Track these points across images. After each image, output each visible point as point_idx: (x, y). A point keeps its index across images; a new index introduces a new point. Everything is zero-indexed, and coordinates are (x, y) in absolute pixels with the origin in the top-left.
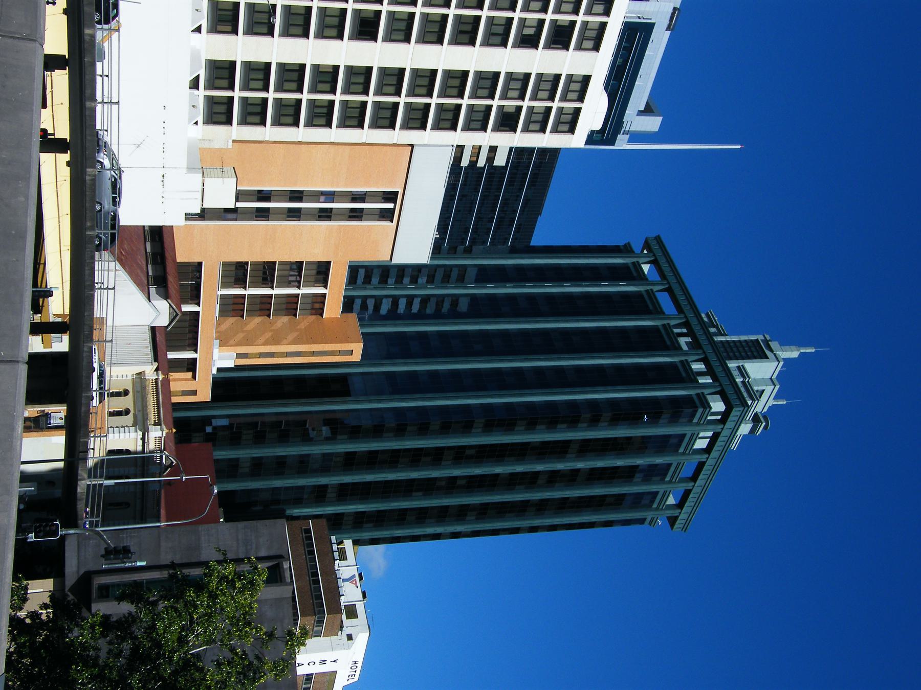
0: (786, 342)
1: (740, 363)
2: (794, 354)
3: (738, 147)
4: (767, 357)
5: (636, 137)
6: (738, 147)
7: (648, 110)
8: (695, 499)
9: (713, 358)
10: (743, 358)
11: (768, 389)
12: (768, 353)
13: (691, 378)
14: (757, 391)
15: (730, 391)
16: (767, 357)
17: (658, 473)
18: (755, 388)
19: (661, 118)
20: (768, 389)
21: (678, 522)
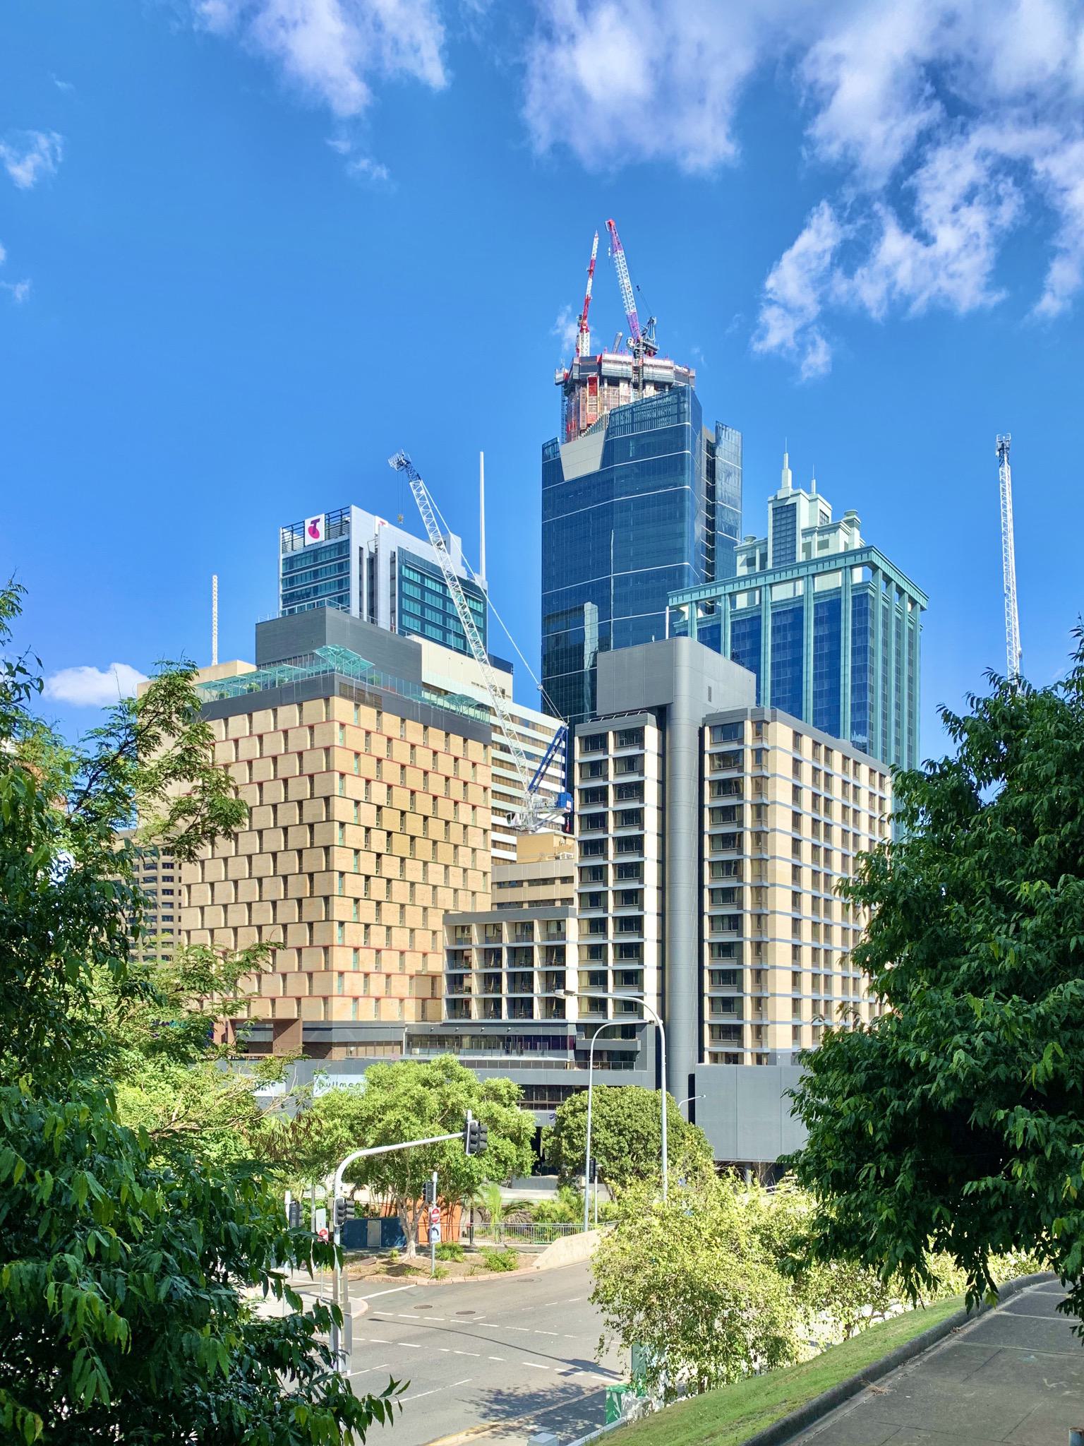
0: (778, 485)
1: (799, 533)
3: (482, 454)
6: (482, 454)
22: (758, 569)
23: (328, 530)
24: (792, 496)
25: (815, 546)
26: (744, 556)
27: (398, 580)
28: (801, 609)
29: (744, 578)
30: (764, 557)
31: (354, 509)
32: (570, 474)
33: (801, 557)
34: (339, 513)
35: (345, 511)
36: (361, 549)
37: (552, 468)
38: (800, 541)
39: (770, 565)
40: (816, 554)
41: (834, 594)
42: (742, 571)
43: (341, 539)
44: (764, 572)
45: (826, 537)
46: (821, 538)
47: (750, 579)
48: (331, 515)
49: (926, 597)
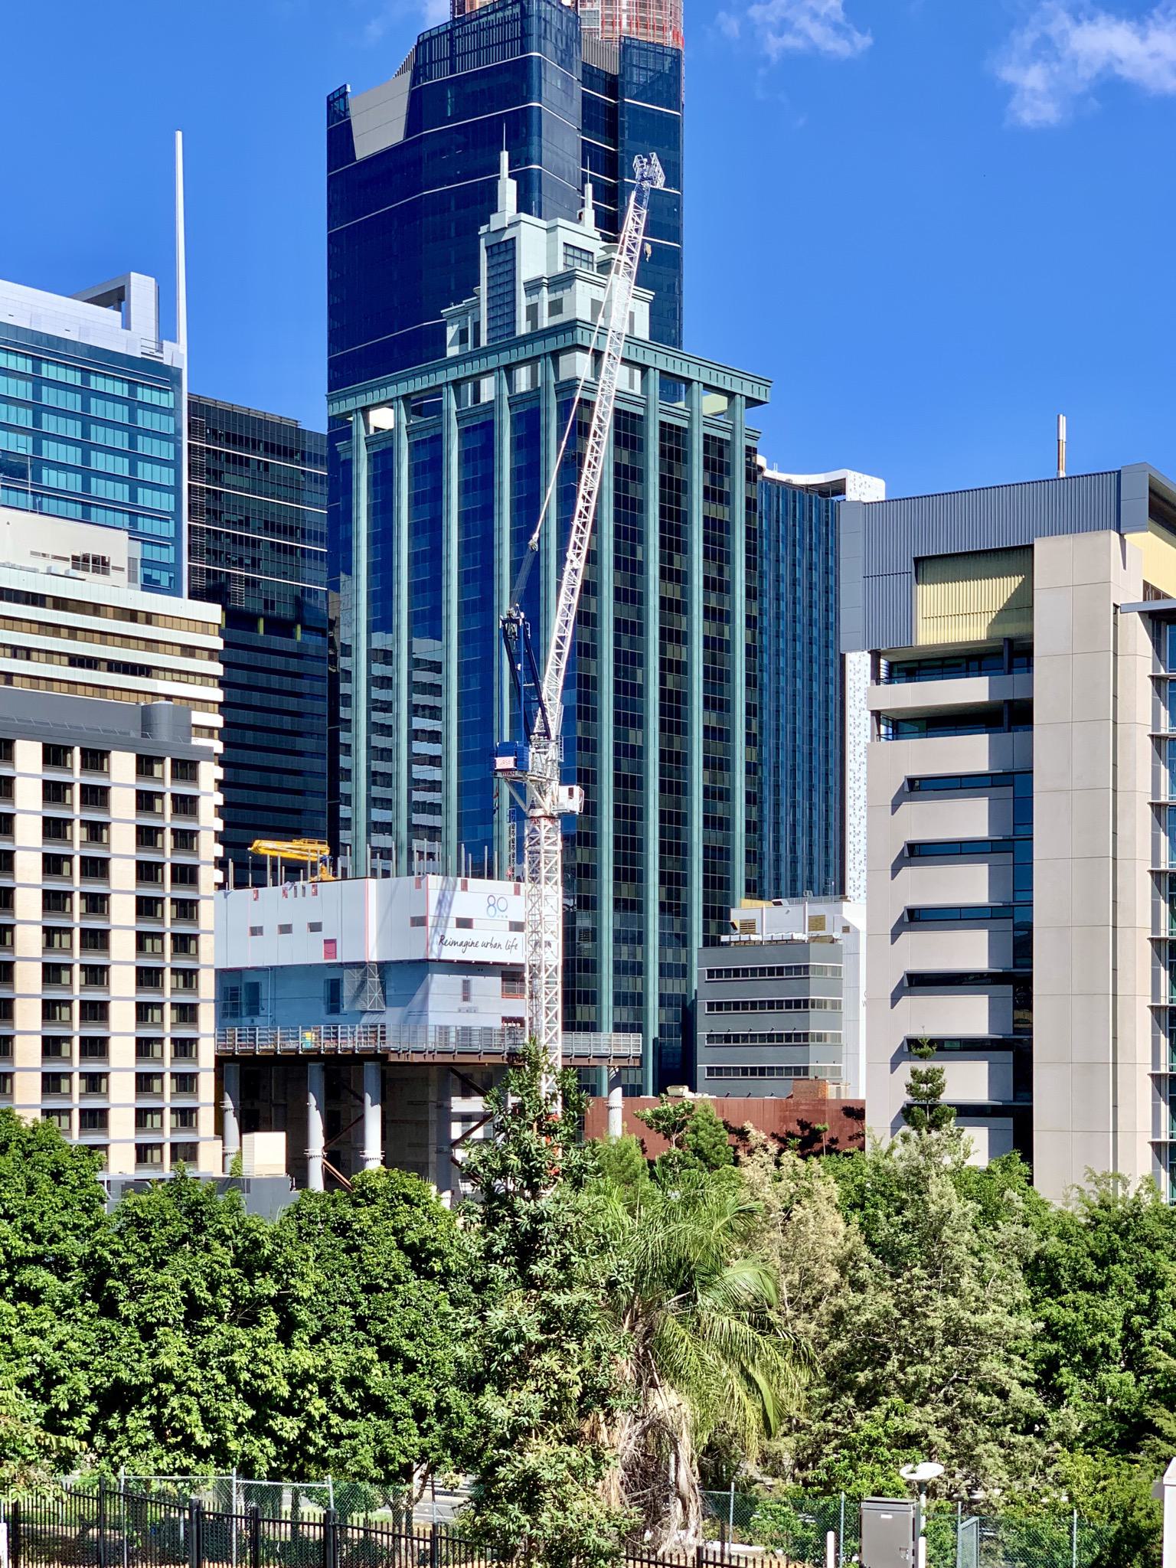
3: (179, 134)
4: (513, 239)
5: (166, 329)
6: (179, 134)
7: (116, 298)
8: (721, 375)
9: (505, 358)
10: (514, 280)
11: (563, 236)
12: (506, 236)
13: (535, 394)
14: (565, 264)
15: (552, 344)
16: (513, 239)
17: (674, 439)
18: (561, 269)
19: (133, 274)
20: (563, 236)
21: (756, 397)
22: (470, 346)
24: (511, 225)
25: (544, 309)
26: (456, 327)
28: (491, 423)
29: (456, 361)
30: (477, 326)
32: (366, 146)
33: (523, 328)
37: (340, 136)
38: (523, 301)
39: (484, 342)
40: (545, 322)
41: (485, 412)
42: (452, 351)
44: (479, 354)
45: (559, 294)
46: (554, 297)
47: (464, 362)
49: (766, 383)
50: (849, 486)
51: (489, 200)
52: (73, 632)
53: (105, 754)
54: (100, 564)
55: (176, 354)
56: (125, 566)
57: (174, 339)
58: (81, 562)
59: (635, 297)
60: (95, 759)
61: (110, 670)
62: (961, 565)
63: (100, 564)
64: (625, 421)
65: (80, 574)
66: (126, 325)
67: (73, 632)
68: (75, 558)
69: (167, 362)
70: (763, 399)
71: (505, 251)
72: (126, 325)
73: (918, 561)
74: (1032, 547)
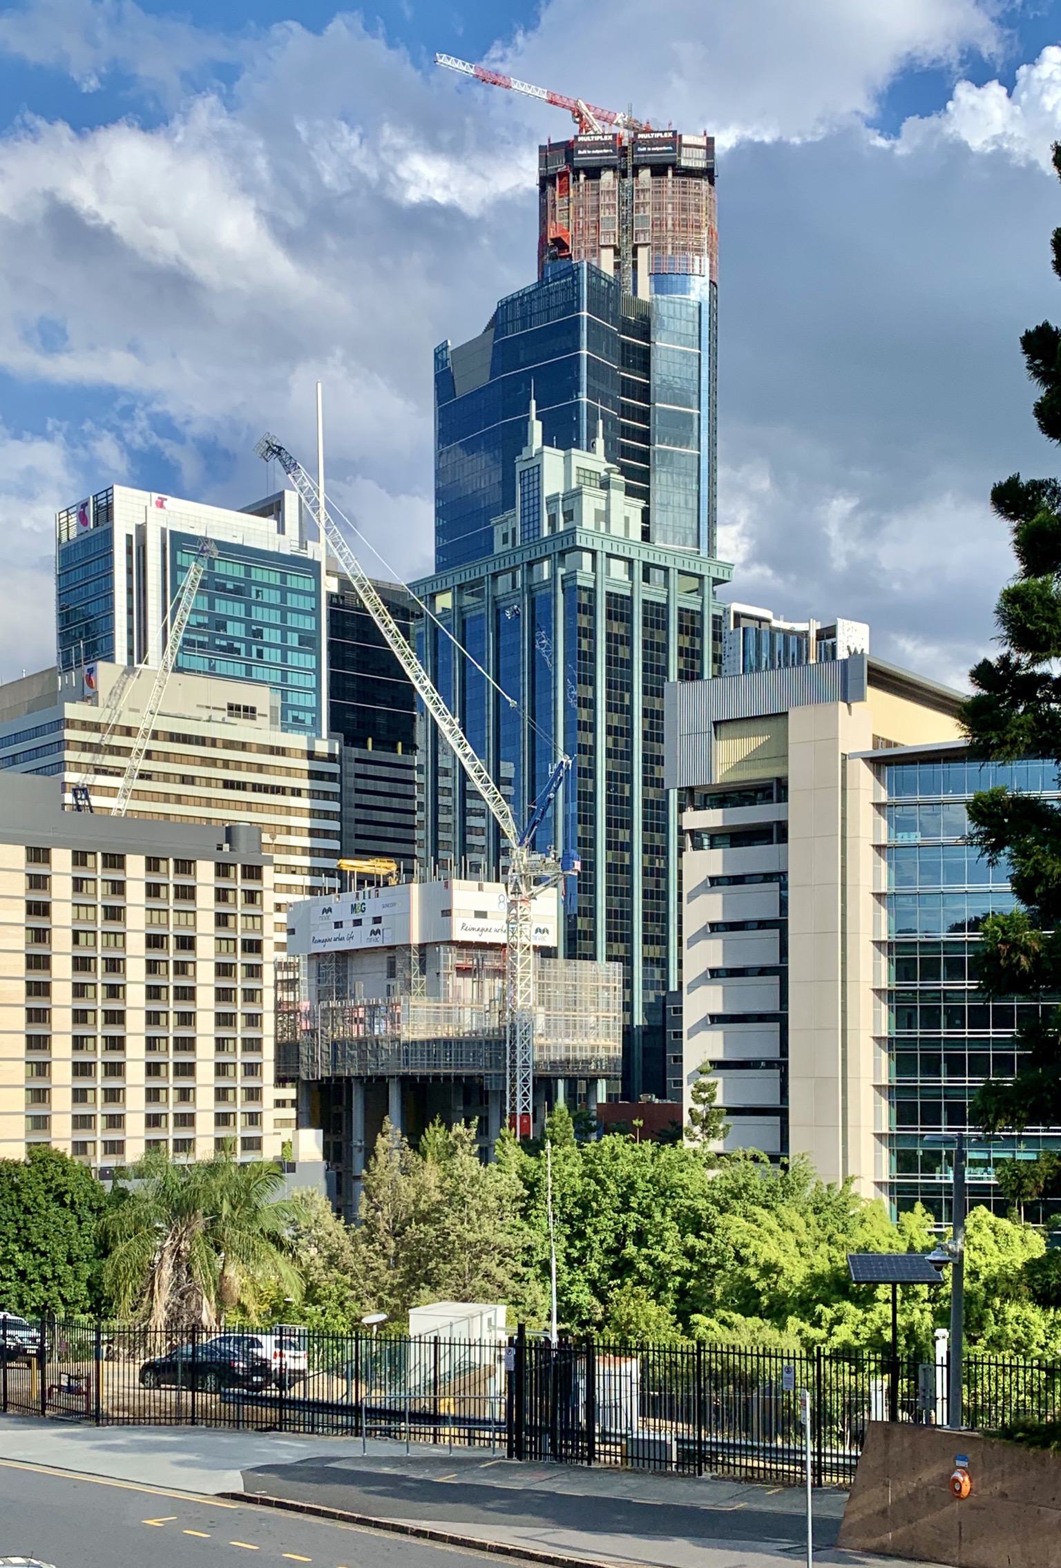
2: (537, 428)
21: (720, 577)
22: (509, 545)
23: (96, 515)
27: (172, 571)
29: (502, 556)
30: (514, 530)
31: (117, 489)
33: (546, 532)
34: (104, 495)
35: (108, 493)
36: (129, 537)
37: (444, 381)
39: (518, 543)
42: (499, 547)
43: (106, 526)
48: (100, 497)
50: (839, 631)
51: (523, 439)
52: (226, 764)
53: (194, 861)
54: (250, 712)
55: (316, 551)
56: (268, 713)
57: (317, 539)
58: (233, 709)
59: (626, 504)
60: (184, 866)
61: (254, 790)
62: (745, 726)
63: (250, 712)
64: (616, 601)
65: (233, 720)
66: (281, 530)
67: (226, 764)
68: (231, 707)
69: (310, 556)
70: (726, 578)
71: (535, 474)
72: (281, 530)
73: (716, 724)
74: (786, 713)
